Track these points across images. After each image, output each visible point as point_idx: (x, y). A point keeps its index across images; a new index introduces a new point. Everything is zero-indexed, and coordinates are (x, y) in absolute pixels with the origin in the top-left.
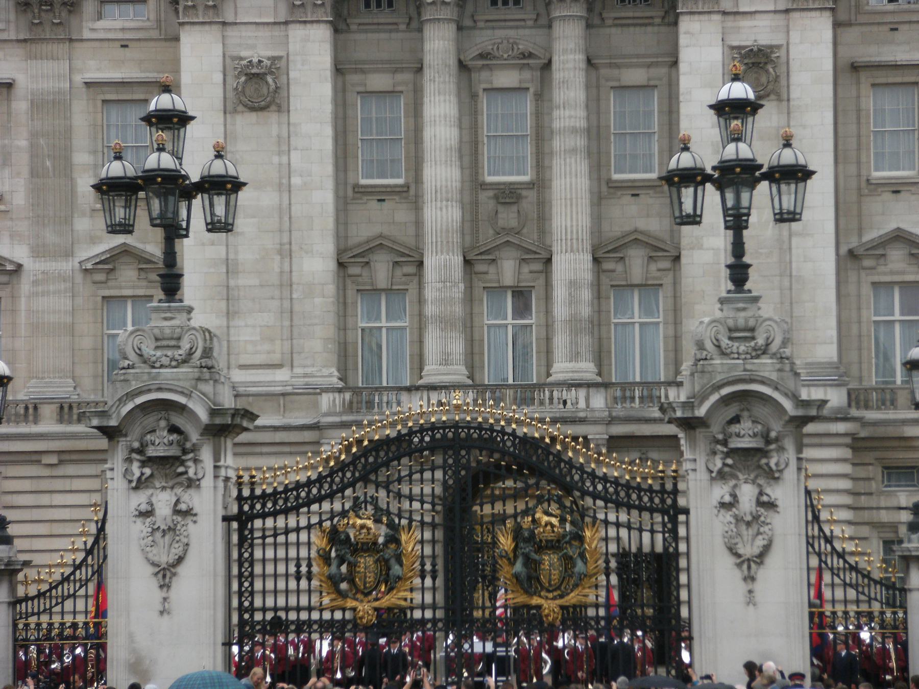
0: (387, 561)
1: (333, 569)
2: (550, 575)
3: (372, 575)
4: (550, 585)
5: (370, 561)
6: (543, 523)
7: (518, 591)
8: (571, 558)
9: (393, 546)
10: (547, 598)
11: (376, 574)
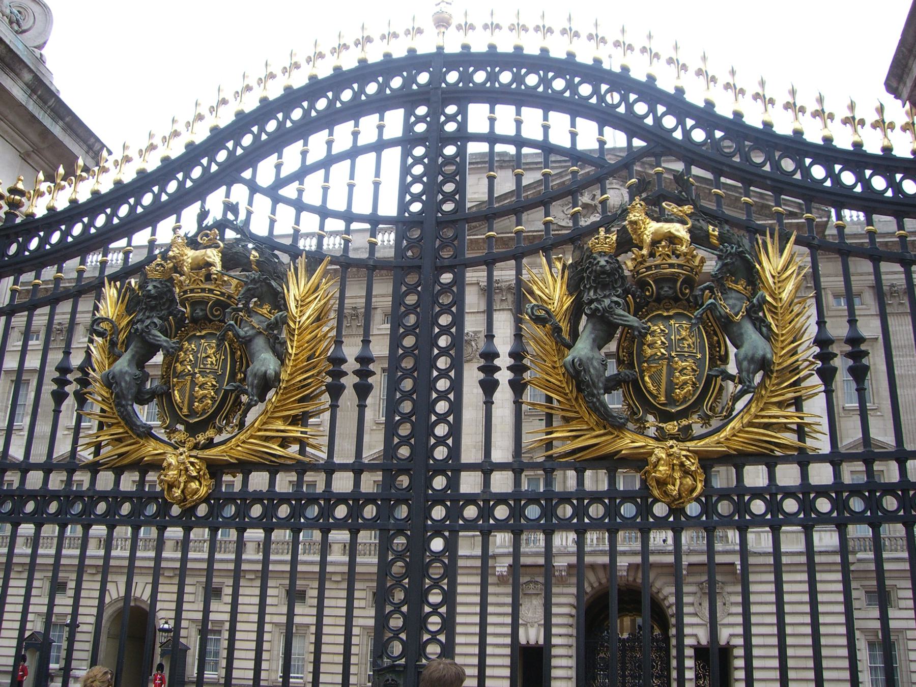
0: (247, 342)
1: (123, 364)
2: (671, 371)
3: (211, 380)
4: (671, 401)
5: (209, 348)
6: (648, 239)
7: (580, 419)
8: (727, 325)
9: (265, 310)
10: (662, 437)
11: (219, 378)
